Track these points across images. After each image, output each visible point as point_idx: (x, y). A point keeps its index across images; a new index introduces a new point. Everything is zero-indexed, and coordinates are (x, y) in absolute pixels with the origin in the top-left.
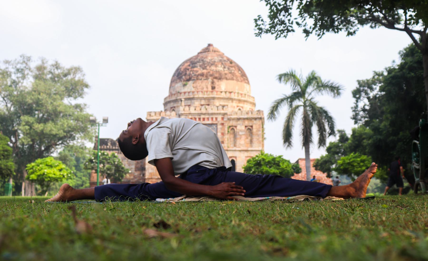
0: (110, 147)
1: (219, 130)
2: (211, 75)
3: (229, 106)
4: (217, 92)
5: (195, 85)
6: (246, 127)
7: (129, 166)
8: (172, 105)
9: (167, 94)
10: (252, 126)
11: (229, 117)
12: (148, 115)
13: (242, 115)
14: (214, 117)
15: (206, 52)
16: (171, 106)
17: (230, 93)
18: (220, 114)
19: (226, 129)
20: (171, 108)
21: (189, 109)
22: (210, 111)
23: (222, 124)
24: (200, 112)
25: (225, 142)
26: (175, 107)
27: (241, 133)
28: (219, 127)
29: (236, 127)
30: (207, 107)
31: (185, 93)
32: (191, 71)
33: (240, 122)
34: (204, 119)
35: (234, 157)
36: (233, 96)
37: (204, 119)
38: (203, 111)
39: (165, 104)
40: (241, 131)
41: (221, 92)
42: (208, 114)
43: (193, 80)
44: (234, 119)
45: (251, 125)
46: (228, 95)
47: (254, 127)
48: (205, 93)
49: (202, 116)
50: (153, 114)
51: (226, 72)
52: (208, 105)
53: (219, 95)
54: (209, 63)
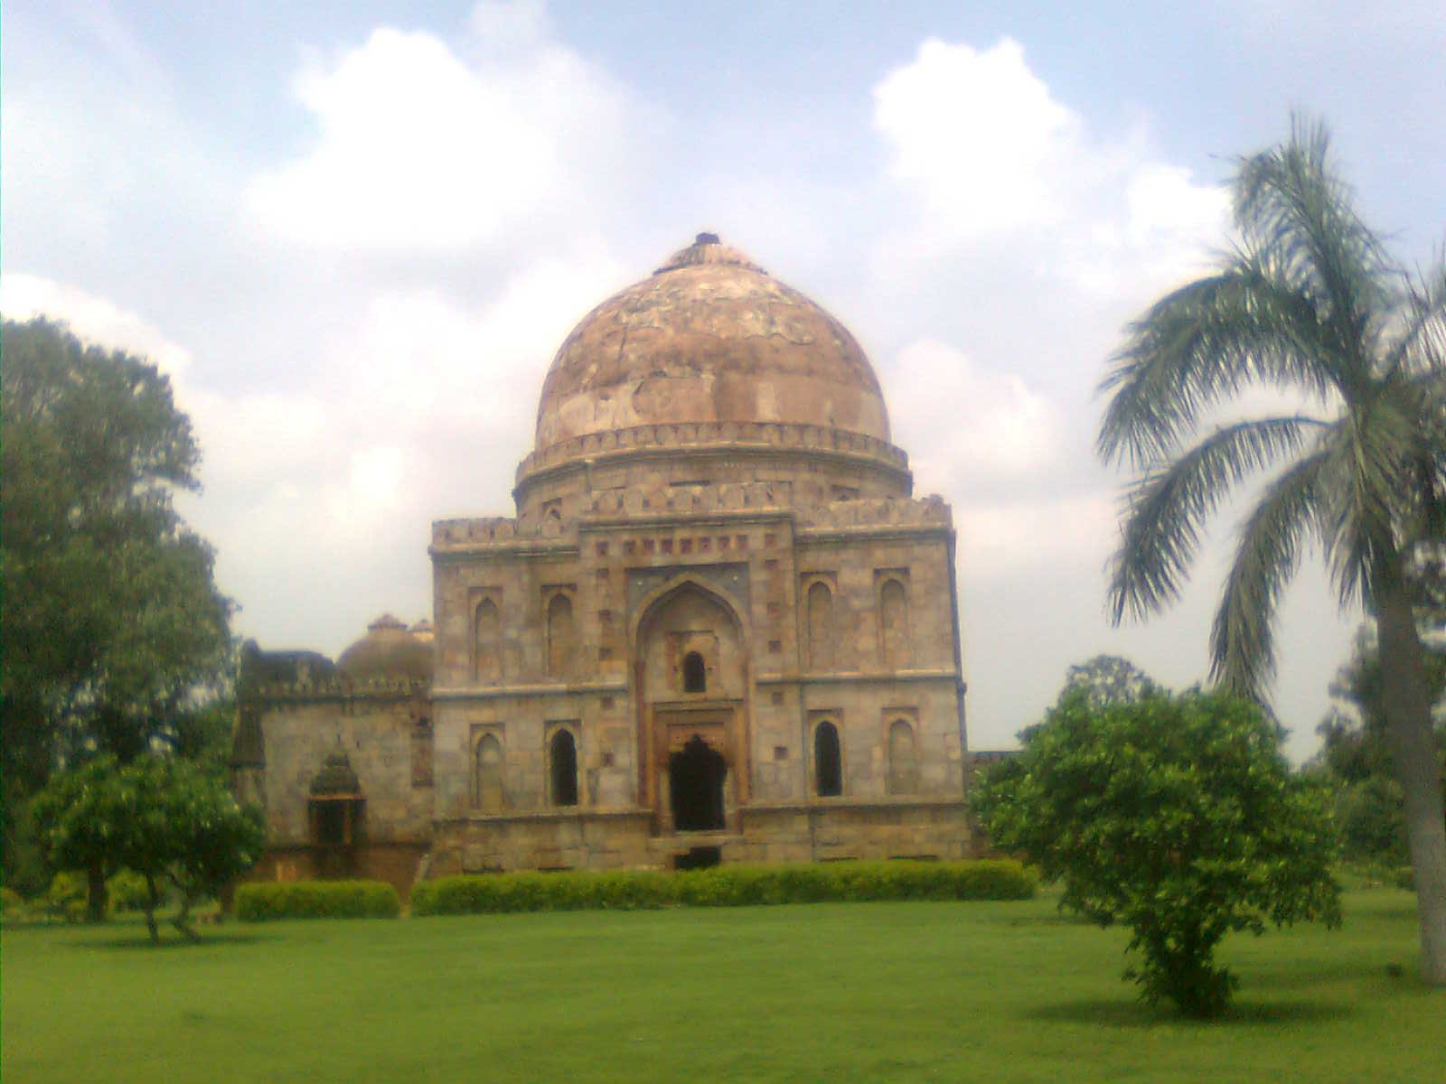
0: (304, 687)
1: (758, 591)
2: (710, 356)
3: (798, 486)
4: (740, 425)
5: (642, 399)
6: (877, 572)
7: (387, 766)
8: (547, 493)
9: (528, 445)
10: (905, 571)
11: (801, 531)
12: (436, 536)
13: (857, 522)
14: (732, 533)
15: (690, 263)
16: (546, 500)
17: (802, 428)
18: (758, 519)
19: (789, 584)
20: (546, 505)
21: (620, 504)
22: (716, 510)
23: (771, 564)
24: (665, 514)
25: (785, 643)
26: (559, 501)
27: (856, 603)
28: (759, 576)
29: (832, 574)
30: (697, 490)
31: (600, 436)
32: (624, 341)
33: (850, 554)
34: (686, 545)
35: (829, 711)
36: (810, 443)
37: (686, 545)
38: (686, 511)
39: (521, 494)
40: (855, 592)
41: (761, 425)
42: (705, 522)
43: (633, 379)
44: (822, 541)
45: (900, 563)
46: (791, 441)
47: (916, 571)
48: (690, 432)
49: (680, 534)
50: (460, 532)
51: (776, 341)
52: (704, 483)
53: (752, 438)
54: (703, 301)
